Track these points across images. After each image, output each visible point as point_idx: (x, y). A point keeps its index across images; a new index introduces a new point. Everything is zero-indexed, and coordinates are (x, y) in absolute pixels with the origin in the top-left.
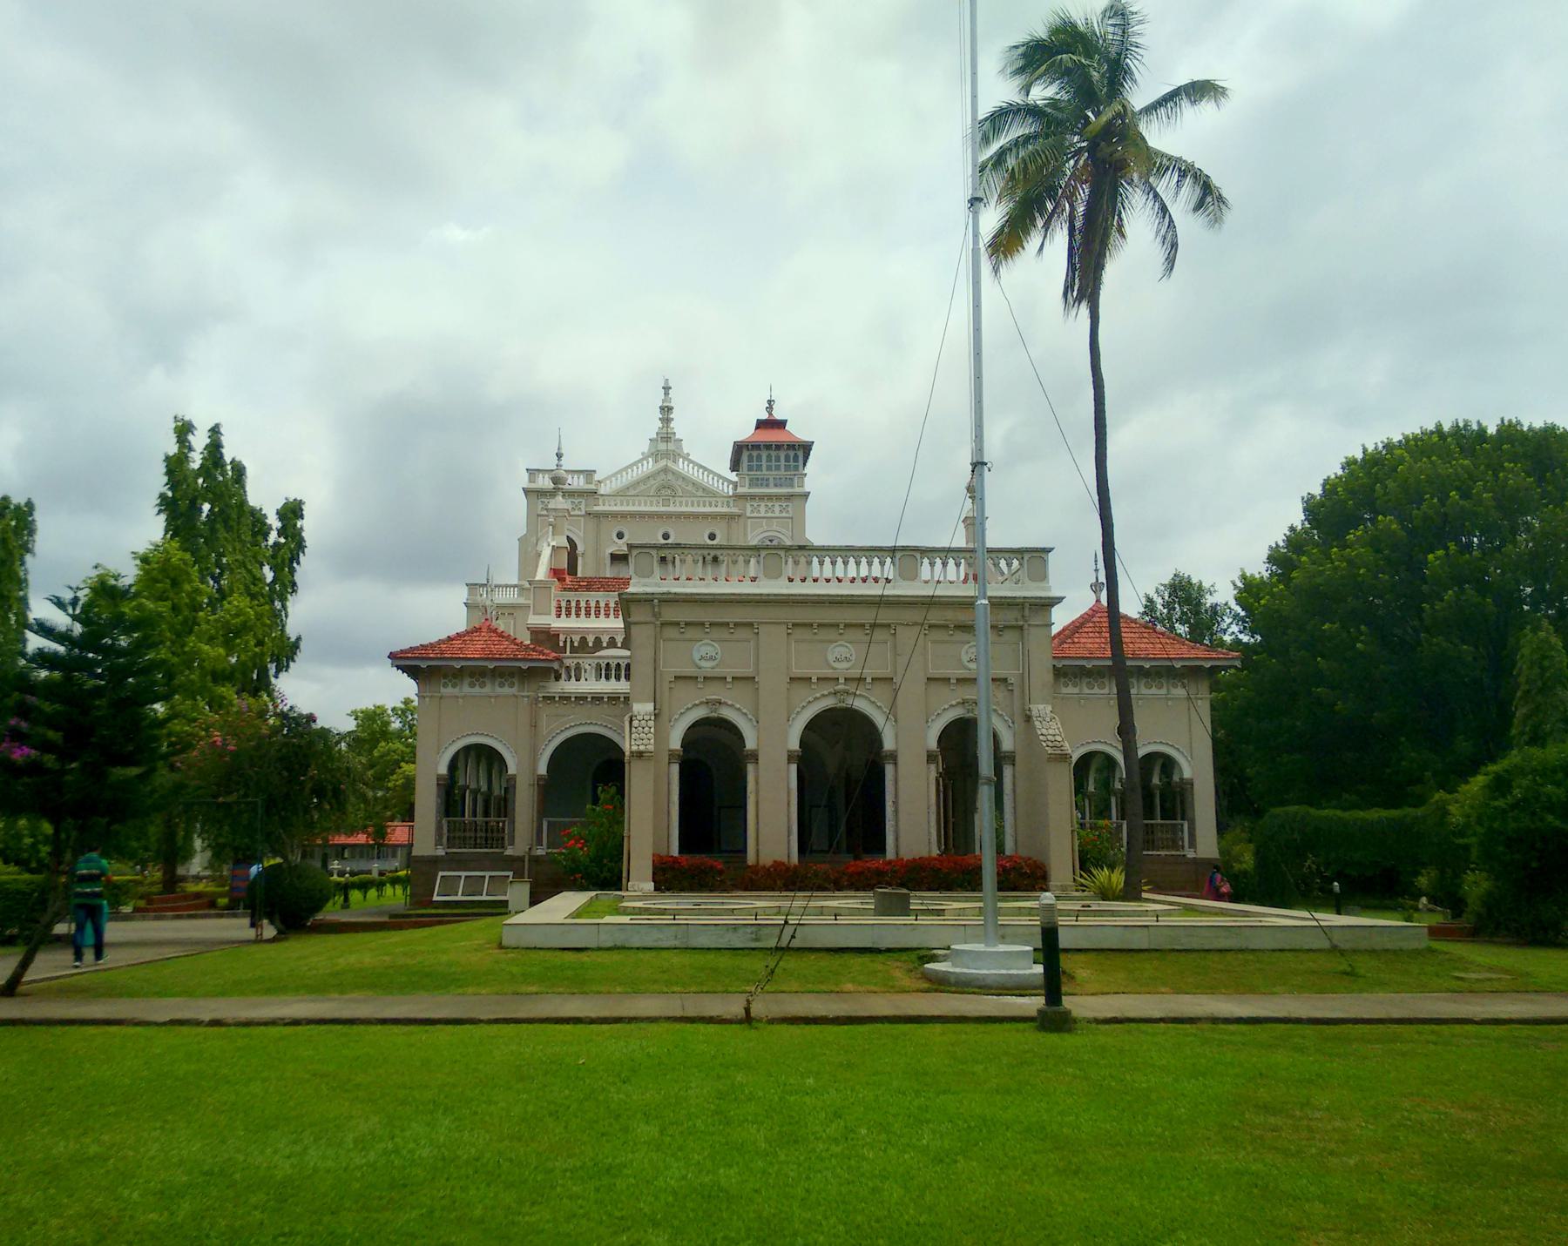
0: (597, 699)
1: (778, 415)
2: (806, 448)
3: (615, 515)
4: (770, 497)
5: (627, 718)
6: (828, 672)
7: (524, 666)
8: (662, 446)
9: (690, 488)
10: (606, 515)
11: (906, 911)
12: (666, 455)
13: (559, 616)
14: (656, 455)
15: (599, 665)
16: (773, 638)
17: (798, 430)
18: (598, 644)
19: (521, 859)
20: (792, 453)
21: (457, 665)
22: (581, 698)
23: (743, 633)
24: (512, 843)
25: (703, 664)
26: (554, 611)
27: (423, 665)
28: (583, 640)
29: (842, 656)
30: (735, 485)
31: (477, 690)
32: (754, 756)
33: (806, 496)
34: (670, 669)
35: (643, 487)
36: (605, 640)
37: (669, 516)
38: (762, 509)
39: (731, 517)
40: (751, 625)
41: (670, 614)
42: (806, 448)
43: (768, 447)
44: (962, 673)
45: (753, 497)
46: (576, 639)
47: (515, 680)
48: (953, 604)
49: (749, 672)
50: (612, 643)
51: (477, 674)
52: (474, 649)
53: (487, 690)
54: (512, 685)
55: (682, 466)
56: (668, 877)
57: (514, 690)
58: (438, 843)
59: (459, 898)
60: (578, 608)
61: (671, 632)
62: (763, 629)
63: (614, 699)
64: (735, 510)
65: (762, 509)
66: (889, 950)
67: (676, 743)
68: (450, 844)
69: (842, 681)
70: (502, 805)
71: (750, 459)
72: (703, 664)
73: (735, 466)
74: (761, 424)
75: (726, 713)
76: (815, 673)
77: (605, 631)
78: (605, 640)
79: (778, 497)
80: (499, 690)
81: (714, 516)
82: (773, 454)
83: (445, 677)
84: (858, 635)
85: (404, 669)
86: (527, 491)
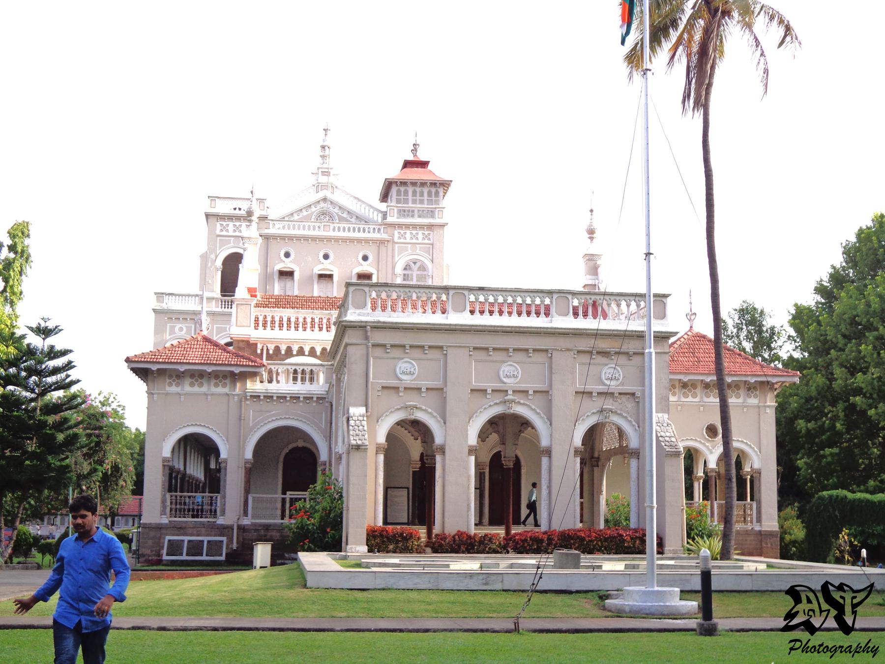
0: (295, 398)
1: (422, 157)
2: (445, 185)
3: (283, 238)
4: (415, 226)
5: (345, 419)
6: (498, 386)
7: (237, 370)
8: (323, 179)
9: (345, 215)
10: (275, 237)
11: (577, 566)
12: (324, 187)
13: (256, 328)
14: (319, 187)
15: (295, 372)
17: (438, 170)
18: (289, 352)
19: (231, 528)
20: (433, 190)
21: (182, 368)
22: (282, 398)
24: (223, 513)
26: (253, 325)
27: (154, 368)
28: (277, 349)
29: (512, 373)
30: (385, 215)
31: (196, 389)
32: (442, 450)
33: (443, 226)
35: (305, 213)
36: (295, 349)
37: (329, 239)
38: (408, 236)
39: (382, 242)
40: (441, 348)
41: (378, 337)
42: (445, 185)
43: (414, 184)
44: (601, 388)
45: (400, 226)
46: (271, 348)
50: (301, 352)
51: (198, 376)
52: (195, 356)
53: (204, 389)
54: (225, 386)
55: (337, 197)
56: (379, 541)
57: (226, 390)
58: (163, 512)
59: (184, 557)
60: (273, 322)
61: (379, 352)
63: (308, 398)
64: (385, 236)
65: (408, 236)
66: (578, 592)
67: (381, 438)
68: (175, 512)
70: (214, 481)
71: (399, 193)
73: (385, 197)
74: (407, 164)
76: (489, 386)
77: (295, 341)
78: (295, 349)
79: (422, 227)
80: (214, 390)
81: (367, 241)
82: (418, 189)
83: (170, 377)
84: (520, 356)
85: (135, 370)
86: (208, 216)
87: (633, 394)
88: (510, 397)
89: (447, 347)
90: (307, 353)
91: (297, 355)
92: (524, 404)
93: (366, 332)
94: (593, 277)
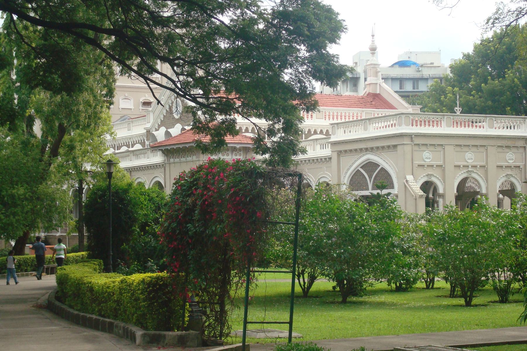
6: (465, 164)
16: (450, 150)
23: (439, 148)
25: (426, 160)
29: (470, 157)
34: (417, 162)
40: (442, 145)
41: (417, 141)
47: (242, 153)
48: (505, 138)
49: (440, 163)
61: (416, 148)
62: (446, 146)
69: (470, 167)
72: (426, 160)
75: (434, 179)
76: (462, 163)
84: (474, 149)
87: (519, 167)
88: (470, 169)
89: (445, 145)
90: (250, 131)
91: (245, 133)
92: (476, 173)
93: (412, 138)
94: (375, 78)
